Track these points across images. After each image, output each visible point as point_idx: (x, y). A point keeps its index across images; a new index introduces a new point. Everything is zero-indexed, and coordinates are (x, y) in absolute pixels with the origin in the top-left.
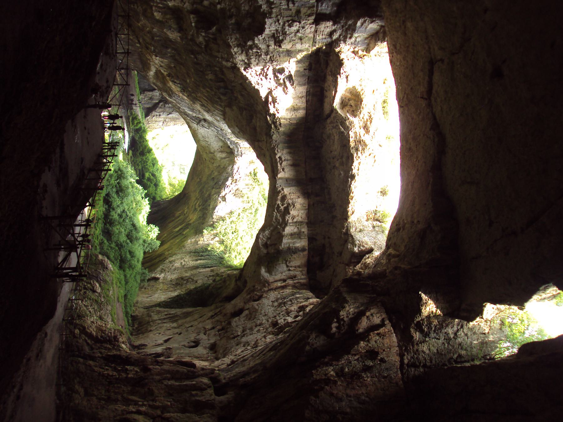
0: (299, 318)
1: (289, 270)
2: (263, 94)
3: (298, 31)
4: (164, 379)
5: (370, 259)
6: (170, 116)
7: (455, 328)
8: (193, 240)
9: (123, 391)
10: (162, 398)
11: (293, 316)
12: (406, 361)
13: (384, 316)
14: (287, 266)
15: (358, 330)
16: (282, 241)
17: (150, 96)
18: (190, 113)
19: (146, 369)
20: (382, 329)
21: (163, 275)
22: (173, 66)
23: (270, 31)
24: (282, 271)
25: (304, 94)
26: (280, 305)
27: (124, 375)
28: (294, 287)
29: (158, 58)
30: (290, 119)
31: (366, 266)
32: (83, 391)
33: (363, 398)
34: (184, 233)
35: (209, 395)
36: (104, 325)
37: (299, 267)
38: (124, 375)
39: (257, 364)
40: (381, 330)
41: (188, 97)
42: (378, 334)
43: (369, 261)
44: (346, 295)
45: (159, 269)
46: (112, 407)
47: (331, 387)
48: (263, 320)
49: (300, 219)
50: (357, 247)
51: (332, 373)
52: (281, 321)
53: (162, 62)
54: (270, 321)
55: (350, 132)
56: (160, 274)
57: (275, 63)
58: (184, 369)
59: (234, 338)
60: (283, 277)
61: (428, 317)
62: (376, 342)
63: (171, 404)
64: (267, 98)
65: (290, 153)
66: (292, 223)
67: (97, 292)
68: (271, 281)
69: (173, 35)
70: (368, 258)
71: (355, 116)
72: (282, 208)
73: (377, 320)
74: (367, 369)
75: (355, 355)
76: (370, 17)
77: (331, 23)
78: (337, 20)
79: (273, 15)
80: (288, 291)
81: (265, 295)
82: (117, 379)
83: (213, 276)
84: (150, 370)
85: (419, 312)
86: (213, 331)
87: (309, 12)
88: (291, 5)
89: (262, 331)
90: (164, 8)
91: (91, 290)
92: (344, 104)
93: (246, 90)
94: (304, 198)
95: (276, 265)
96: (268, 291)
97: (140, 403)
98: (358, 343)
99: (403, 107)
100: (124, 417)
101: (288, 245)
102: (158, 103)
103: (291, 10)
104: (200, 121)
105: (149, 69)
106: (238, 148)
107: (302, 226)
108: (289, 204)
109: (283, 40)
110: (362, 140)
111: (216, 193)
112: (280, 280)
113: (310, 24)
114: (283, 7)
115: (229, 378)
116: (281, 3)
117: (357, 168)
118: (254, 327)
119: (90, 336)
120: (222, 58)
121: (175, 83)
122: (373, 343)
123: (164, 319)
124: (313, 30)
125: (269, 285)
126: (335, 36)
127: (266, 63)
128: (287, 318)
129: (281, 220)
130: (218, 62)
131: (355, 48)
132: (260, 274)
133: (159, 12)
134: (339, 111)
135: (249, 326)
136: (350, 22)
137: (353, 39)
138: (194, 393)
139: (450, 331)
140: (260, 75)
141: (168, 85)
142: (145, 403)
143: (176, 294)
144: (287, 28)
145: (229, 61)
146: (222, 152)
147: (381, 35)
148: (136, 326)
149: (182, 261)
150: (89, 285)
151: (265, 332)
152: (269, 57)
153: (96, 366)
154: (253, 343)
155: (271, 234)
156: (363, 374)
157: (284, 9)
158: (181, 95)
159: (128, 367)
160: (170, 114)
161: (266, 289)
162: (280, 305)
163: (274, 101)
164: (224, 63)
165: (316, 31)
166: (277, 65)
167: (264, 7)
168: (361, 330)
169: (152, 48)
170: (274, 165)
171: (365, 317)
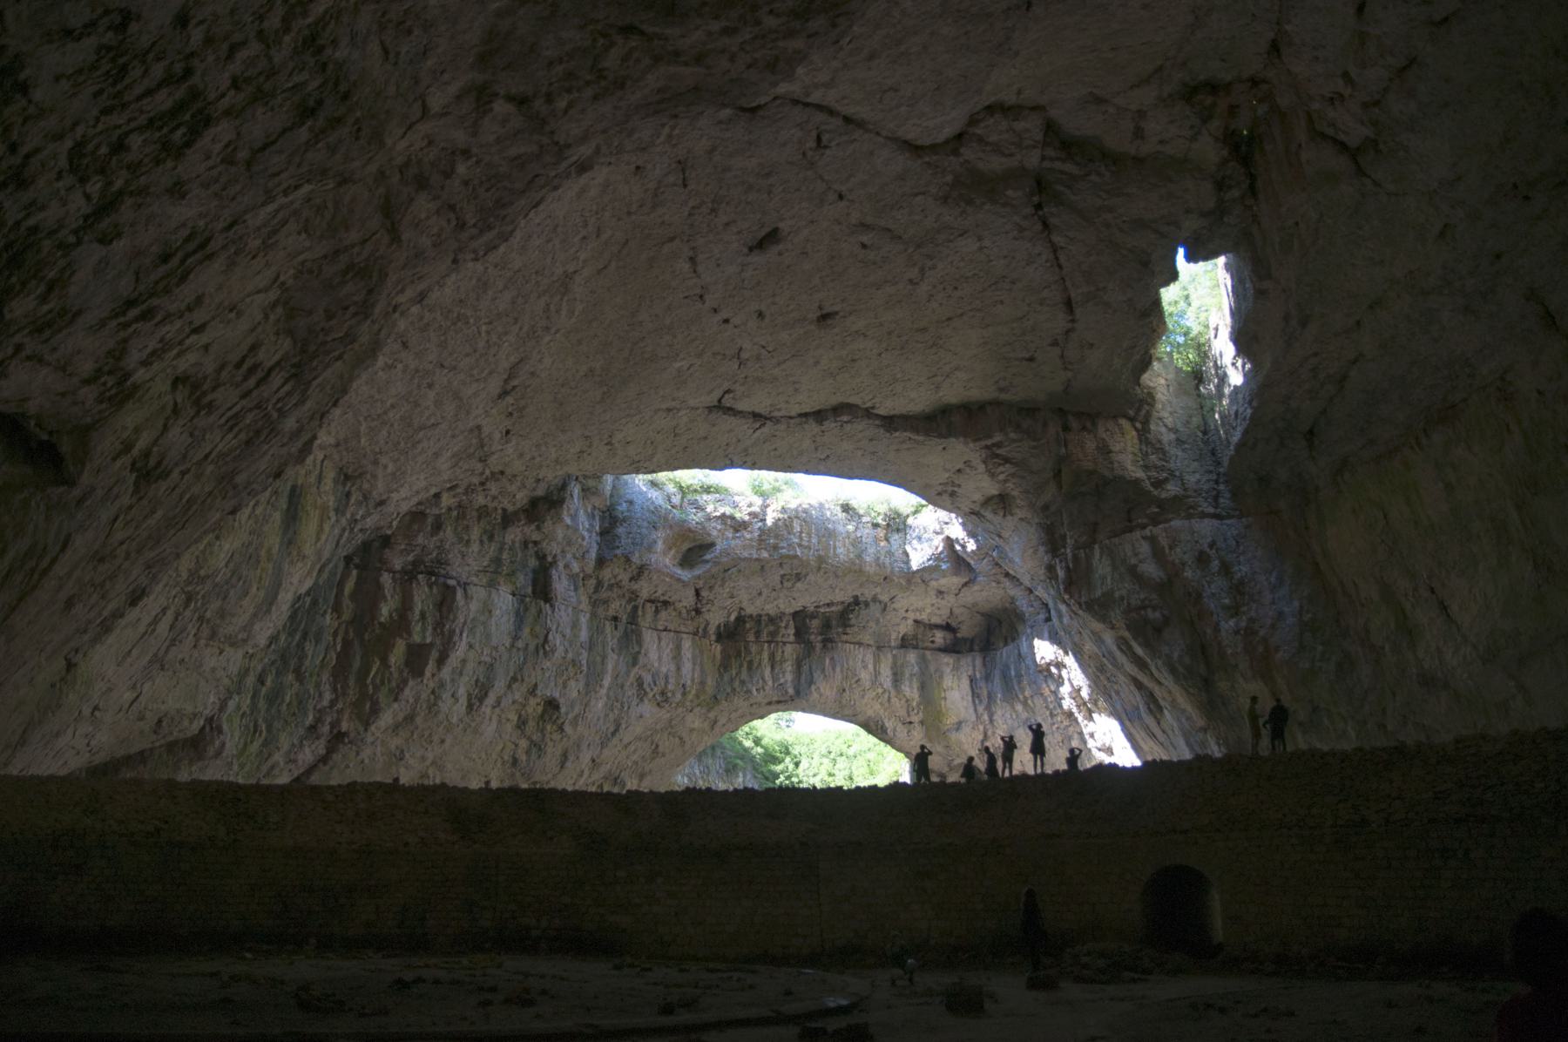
7: (1163, 430)
12: (1211, 510)
13: (1138, 534)
28: (988, 677)
33: (1273, 579)
40: (1164, 542)
44: (1099, 593)
51: (1231, 623)
61: (1146, 468)
71: (712, 545)
73: (1145, 548)
74: (1226, 569)
78: (550, 559)
85: (1137, 482)
101: (915, 685)
139: (1167, 437)
168: (1162, 574)
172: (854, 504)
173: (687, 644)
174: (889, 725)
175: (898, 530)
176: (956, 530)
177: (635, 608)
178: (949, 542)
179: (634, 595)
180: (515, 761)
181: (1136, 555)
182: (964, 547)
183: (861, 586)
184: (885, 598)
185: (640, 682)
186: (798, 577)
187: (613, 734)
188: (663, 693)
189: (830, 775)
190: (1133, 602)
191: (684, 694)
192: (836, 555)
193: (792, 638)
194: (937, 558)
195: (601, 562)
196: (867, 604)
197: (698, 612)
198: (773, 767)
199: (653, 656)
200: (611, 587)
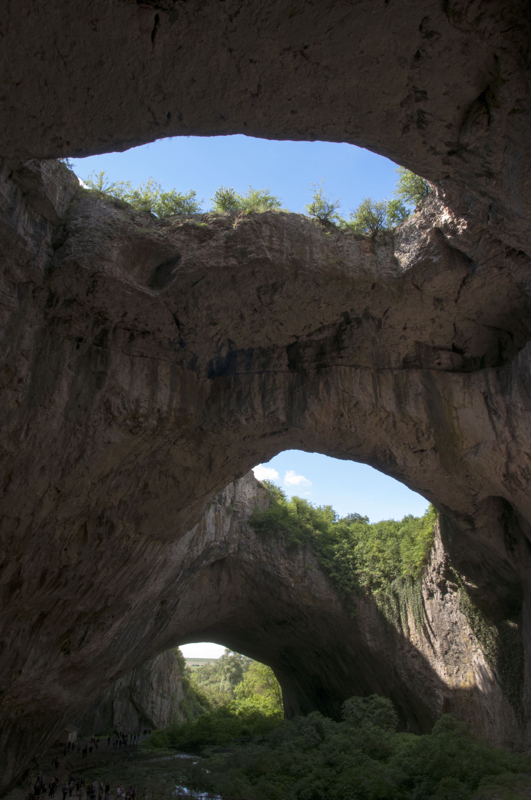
6: (155, 685)
8: (368, 636)
18: (148, 628)
21: (437, 692)
29: (24, 671)
50: (431, 257)
53: (35, 662)
56: (438, 697)
68: (494, 438)
93: (108, 476)
102: (134, 703)
110: (226, 242)
117: (278, 255)
120: (32, 514)
121: (83, 639)
131: (47, 243)
137: (28, 239)
145: (41, 500)
146: (219, 580)
149: (409, 655)
158: (110, 633)
160: (151, 685)
173: (164, 371)
174: (397, 453)
175: (386, 244)
177: (105, 332)
178: (439, 232)
179: (101, 318)
182: (454, 232)
184: (377, 313)
185: (107, 406)
186: (275, 288)
187: (77, 460)
188: (134, 418)
189: (381, 551)
191: (161, 420)
193: (285, 368)
194: (424, 250)
195: (50, 271)
196: (359, 322)
197: (182, 344)
198: (330, 547)
199: (123, 379)
200: (69, 303)
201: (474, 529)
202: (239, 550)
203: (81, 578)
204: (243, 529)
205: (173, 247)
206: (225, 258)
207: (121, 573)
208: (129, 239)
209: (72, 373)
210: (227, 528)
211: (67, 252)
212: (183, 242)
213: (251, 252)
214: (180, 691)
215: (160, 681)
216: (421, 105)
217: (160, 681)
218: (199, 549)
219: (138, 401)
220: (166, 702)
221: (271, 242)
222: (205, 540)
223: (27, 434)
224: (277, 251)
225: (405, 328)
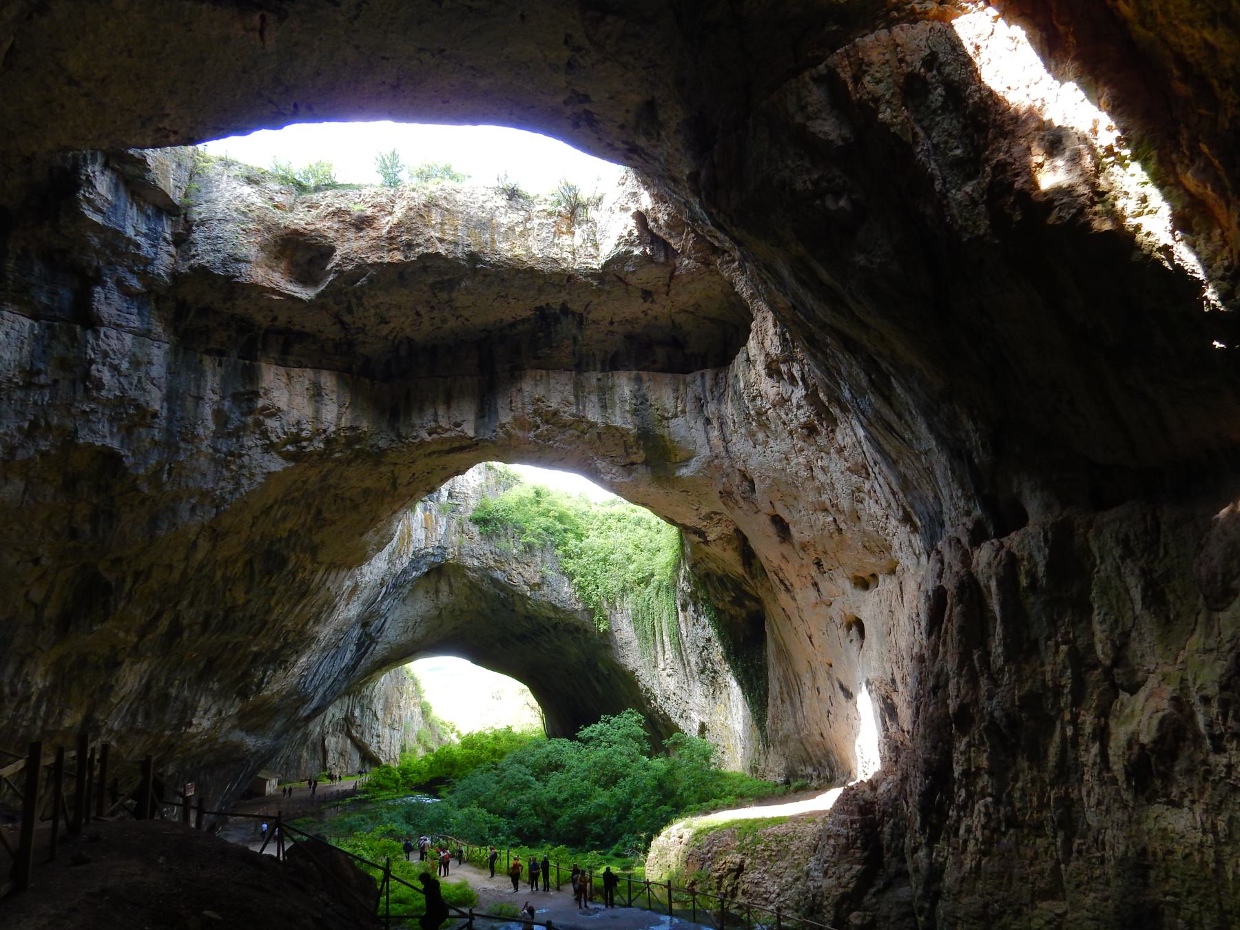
0: (796, 370)
1: (684, 412)
2: (276, 464)
3: (115, 369)
4: (988, 667)
5: (660, 215)
6: (380, 714)
9: (1033, 781)
10: (1048, 668)
11: (790, 388)
13: (807, 75)
14: (676, 416)
15: (844, 139)
16: (616, 428)
17: (337, 756)
19: (963, 718)
20: (842, 75)
21: (693, 715)
22: (216, 686)
23: (111, 433)
24: (685, 429)
25: (282, 370)
26: (764, 426)
27: (984, 780)
30: (340, 407)
31: (675, 225)
32: (1045, 905)
34: (606, 672)
35: (1030, 541)
36: (832, 842)
37: (676, 390)
38: (984, 780)
39: (931, 427)
40: (846, 75)
41: (299, 653)
42: (857, 79)
43: (663, 217)
45: (682, 724)
46: (1092, 818)
47: (1017, 175)
48: (798, 464)
49: (569, 388)
52: (803, 415)
54: (800, 444)
55: (369, 262)
57: (201, 431)
58: (954, 612)
59: (840, 530)
60: (700, 425)
62: (879, 81)
63: (1065, 643)
64: (288, 457)
65: (421, 410)
66: (578, 405)
67: (743, 861)
69: (130, 679)
70: (656, 220)
71: (332, 250)
72: (544, 428)
73: (817, 96)
75: (915, 135)
76: (78, 187)
77: (98, 289)
79: (69, 424)
80: (729, 410)
81: (739, 465)
82: (997, 801)
83: (695, 605)
84: (962, 708)
86: (820, 586)
87: (64, 339)
88: (43, 379)
89: (825, 463)
90: (49, 700)
91: (736, 877)
92: (305, 279)
93: (271, 507)
94: (521, 378)
95: (672, 442)
96: (730, 458)
97: (1069, 731)
98: (885, 126)
99: (295, 106)
100: (1121, 778)
101: (628, 415)
103: (56, 382)
104: (368, 635)
105: (237, 747)
106: (428, 554)
107: (585, 383)
108: (535, 411)
109: (138, 407)
110: (389, 232)
111: (524, 605)
112: (707, 433)
113: (97, 338)
114: (46, 399)
115: (968, 499)
116: (35, 403)
117: (451, 247)
118: (817, 483)
119: (864, 880)
120: (187, 558)
122: (880, 89)
123: (793, 704)
124: (113, 333)
125: (717, 457)
126: (135, 283)
127: (199, 451)
128: (794, 401)
129: (571, 432)
130: (199, 569)
131: (165, 239)
132: (692, 479)
133: (61, 714)
134: (322, 288)
135: (812, 497)
136: (95, 241)
137: (141, 240)
138: (1024, 582)
140: (232, 470)
141: (276, 700)
142: (1068, 717)
143: (733, 683)
144: (103, 393)
146: (437, 592)
147: (129, 168)
148: (810, 770)
150: (726, 882)
151: (828, 453)
152: (182, 445)
153: (961, 864)
154: (854, 478)
155: (604, 456)
156: (971, 101)
157: (51, 398)
159: (957, 771)
160: (375, 714)
161: (726, 463)
162: (764, 426)
163: (296, 439)
164: (200, 556)
165: (118, 327)
166: (206, 427)
167: (44, 446)
168: (846, 132)
169: (167, 733)
170: (446, 447)
171: (809, 123)
172: (523, 188)
176: (646, 201)
180: (74, 534)
181: (803, 108)
183: (540, 290)
184: (576, 307)
190: (799, 186)
191: (328, 441)
192: (495, 252)
196: (557, 319)
201: (706, 542)
202: (460, 554)
203: (252, 617)
204: (465, 528)
205: (325, 237)
206: (390, 251)
207: (299, 607)
208: (269, 229)
209: (216, 398)
210: (441, 531)
211: (193, 252)
212: (337, 231)
213: (419, 245)
214: (418, 718)
215: (387, 707)
216: (587, 106)
217: (387, 707)
218: (406, 561)
219: (299, 423)
220: (397, 735)
221: (443, 232)
222: (412, 549)
223: (169, 474)
224: (450, 243)
225: (612, 323)
